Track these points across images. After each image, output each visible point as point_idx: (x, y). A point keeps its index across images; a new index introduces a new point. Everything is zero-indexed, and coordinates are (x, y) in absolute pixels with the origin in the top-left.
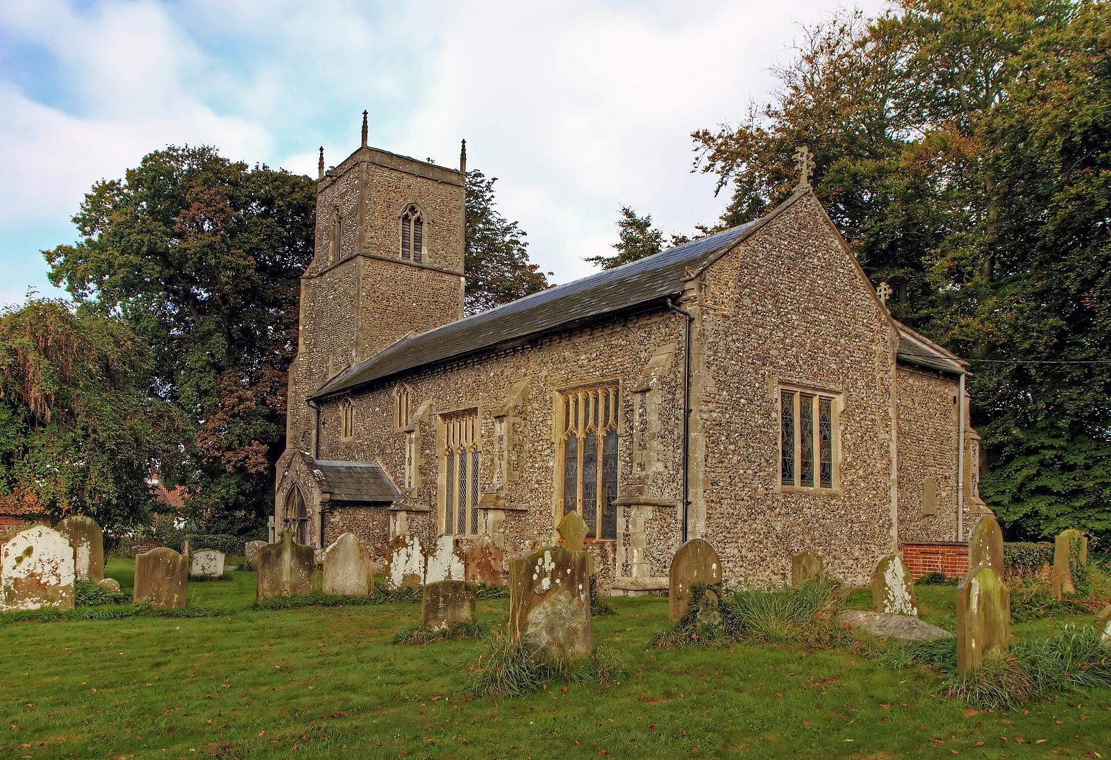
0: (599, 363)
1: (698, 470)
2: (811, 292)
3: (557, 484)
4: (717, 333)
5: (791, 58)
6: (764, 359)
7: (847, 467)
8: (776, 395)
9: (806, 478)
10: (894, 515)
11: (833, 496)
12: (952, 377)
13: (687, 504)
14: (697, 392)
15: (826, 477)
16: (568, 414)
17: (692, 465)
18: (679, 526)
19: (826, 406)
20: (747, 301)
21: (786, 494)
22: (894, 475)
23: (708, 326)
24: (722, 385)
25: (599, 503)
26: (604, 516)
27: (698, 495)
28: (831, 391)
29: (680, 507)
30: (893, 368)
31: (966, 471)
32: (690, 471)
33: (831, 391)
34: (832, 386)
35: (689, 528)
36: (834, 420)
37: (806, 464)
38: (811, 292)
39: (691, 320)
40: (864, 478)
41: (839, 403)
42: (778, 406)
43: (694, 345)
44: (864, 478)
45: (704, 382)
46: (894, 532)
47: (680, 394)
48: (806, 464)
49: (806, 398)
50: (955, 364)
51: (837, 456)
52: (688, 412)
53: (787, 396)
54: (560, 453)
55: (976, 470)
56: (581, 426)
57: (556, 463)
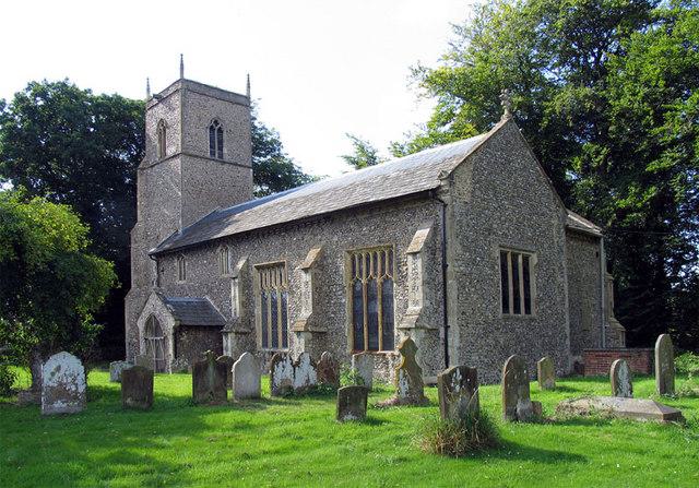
0: (377, 233)
1: (453, 305)
2: (515, 185)
3: (348, 314)
4: (461, 215)
5: (466, 17)
6: (490, 231)
7: (540, 301)
8: (498, 255)
9: (517, 310)
10: (568, 331)
11: (532, 320)
12: (594, 239)
13: (447, 328)
14: (449, 253)
15: (528, 310)
16: (354, 266)
17: (450, 302)
18: (442, 342)
19: (526, 260)
20: (478, 193)
21: (506, 319)
22: (567, 305)
23: (456, 210)
24: (466, 248)
25: (380, 327)
26: (383, 335)
27: (453, 321)
28: (530, 251)
29: (442, 330)
30: (564, 238)
31: (606, 302)
32: (448, 306)
33: (530, 251)
34: (529, 248)
35: (449, 344)
36: (531, 270)
37: (517, 299)
38: (515, 185)
39: (445, 206)
40: (550, 308)
41: (534, 260)
42: (499, 261)
43: (448, 222)
44: (550, 308)
45: (455, 247)
46: (568, 342)
47: (439, 256)
48: (517, 299)
49: (515, 257)
50: (597, 231)
51: (534, 294)
52: (445, 266)
53: (503, 255)
54: (349, 294)
55: (612, 300)
56: (364, 275)
57: (347, 300)
